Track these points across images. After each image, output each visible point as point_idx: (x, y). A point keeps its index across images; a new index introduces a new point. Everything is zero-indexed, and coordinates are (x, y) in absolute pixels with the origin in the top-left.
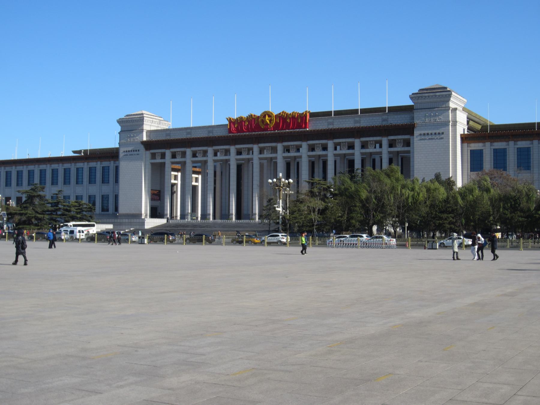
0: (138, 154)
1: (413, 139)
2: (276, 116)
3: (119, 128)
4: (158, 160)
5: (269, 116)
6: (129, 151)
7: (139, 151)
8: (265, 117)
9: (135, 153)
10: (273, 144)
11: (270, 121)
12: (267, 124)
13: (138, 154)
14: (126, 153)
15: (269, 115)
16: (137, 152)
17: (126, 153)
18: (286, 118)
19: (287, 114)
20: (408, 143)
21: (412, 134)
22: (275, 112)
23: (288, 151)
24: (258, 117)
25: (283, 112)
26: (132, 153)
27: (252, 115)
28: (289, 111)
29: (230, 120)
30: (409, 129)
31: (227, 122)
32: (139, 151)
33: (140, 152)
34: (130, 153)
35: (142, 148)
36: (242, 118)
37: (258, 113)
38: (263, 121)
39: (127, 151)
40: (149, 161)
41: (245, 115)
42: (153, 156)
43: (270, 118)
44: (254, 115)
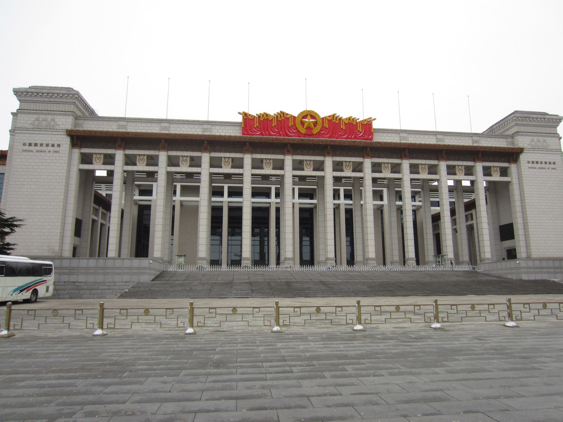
0: (56, 152)
1: (519, 169)
2: (323, 118)
3: (15, 104)
5: (313, 117)
6: (36, 145)
7: (59, 146)
8: (305, 117)
9: (50, 148)
10: (280, 157)
11: (315, 124)
13: (56, 152)
15: (313, 115)
16: (56, 148)
17: (27, 148)
18: (339, 124)
19: (340, 119)
20: (504, 172)
22: (323, 113)
23: (489, 175)
24: (294, 117)
25: (334, 116)
27: (281, 112)
28: (344, 115)
29: (245, 115)
30: (512, 155)
31: (239, 119)
32: (59, 146)
33: (61, 149)
34: (38, 148)
35: (66, 141)
36: (267, 115)
37: (295, 111)
38: (303, 123)
39: (30, 145)
40: (77, 166)
41: (272, 111)
42: (86, 159)
44: (287, 114)
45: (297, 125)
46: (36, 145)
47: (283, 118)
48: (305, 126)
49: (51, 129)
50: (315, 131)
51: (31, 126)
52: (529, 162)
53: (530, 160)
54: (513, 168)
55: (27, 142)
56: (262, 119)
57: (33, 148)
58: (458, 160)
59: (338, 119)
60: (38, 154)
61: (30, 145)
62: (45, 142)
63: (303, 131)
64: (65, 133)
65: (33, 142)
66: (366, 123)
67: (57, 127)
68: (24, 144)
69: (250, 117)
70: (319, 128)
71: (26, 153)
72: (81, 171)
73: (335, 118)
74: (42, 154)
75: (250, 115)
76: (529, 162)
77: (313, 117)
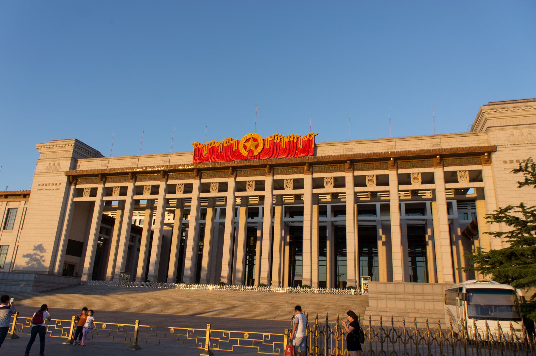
4: (86, 198)
6: (46, 185)
7: (60, 184)
9: (55, 187)
12: (251, 151)
14: (40, 187)
16: (58, 187)
17: (40, 187)
20: (476, 177)
21: (488, 161)
26: (51, 187)
32: (60, 184)
34: (47, 187)
38: (245, 147)
39: (43, 185)
43: (256, 143)
45: (240, 149)
46: (46, 185)
47: (228, 144)
48: (247, 149)
49: (57, 171)
50: (256, 153)
51: (45, 171)
52: (505, 162)
53: (508, 159)
54: (486, 171)
55: (41, 183)
56: (210, 147)
57: (44, 187)
58: (413, 167)
59: (279, 138)
60: (47, 191)
61: (43, 185)
62: (51, 182)
63: (245, 153)
64: (64, 174)
65: (45, 183)
66: (307, 139)
67: (60, 170)
68: (39, 185)
69: (200, 147)
70: (260, 149)
71: (39, 192)
72: (75, 204)
73: (276, 137)
74: (49, 191)
75: (200, 144)
76: (505, 162)
77: (255, 140)
